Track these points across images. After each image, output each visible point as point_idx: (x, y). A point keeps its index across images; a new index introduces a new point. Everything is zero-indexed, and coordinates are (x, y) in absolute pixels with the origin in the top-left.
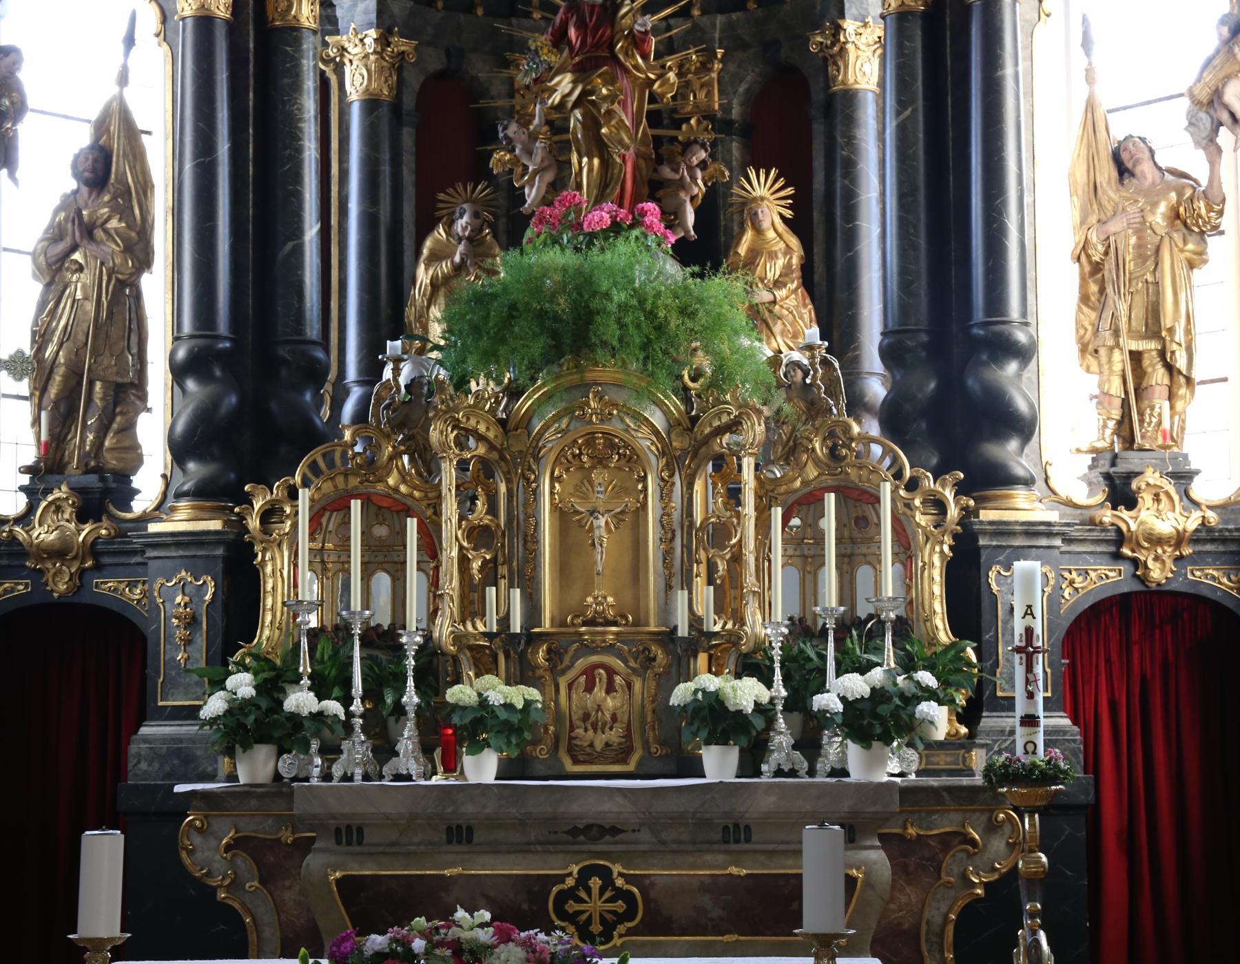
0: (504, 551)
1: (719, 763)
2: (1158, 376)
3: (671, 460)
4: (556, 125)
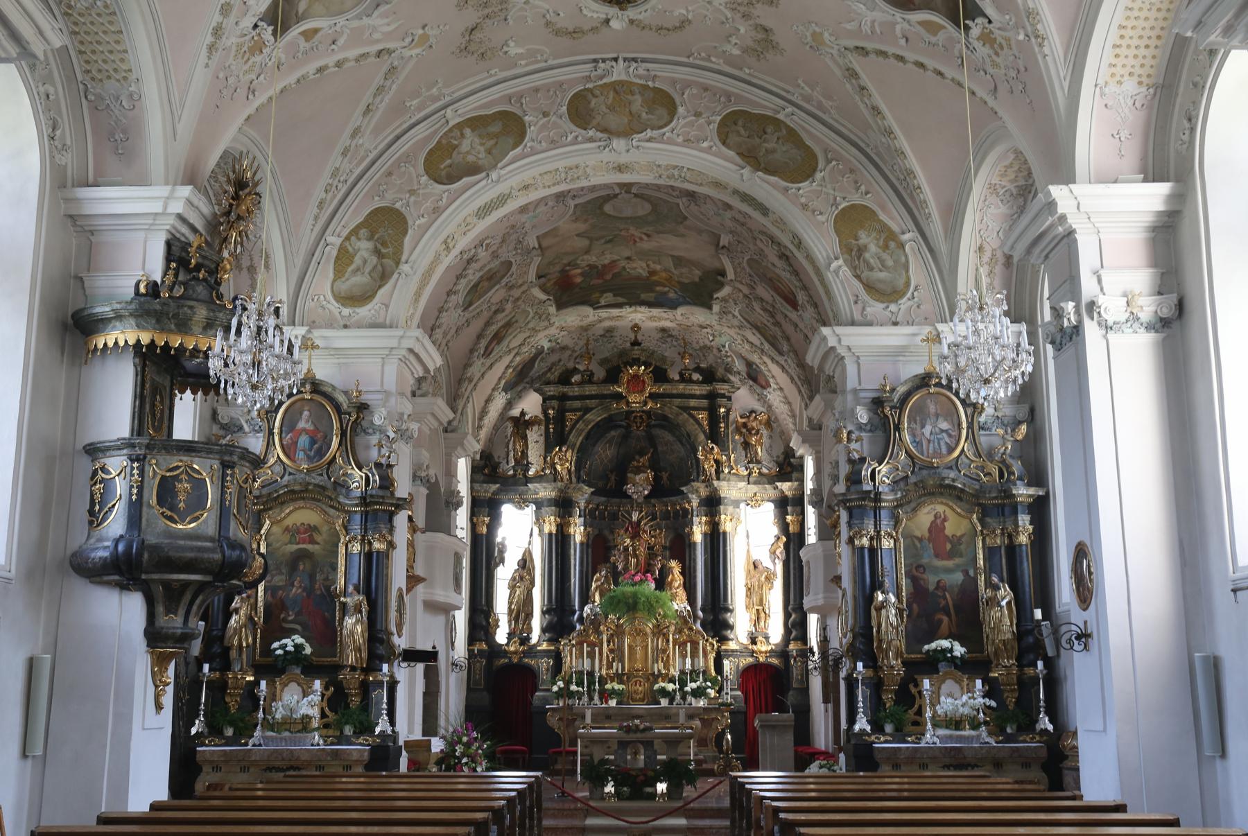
0: (617, 654)
1: (664, 702)
2: (762, 615)
3: (654, 634)
4: (626, 549)
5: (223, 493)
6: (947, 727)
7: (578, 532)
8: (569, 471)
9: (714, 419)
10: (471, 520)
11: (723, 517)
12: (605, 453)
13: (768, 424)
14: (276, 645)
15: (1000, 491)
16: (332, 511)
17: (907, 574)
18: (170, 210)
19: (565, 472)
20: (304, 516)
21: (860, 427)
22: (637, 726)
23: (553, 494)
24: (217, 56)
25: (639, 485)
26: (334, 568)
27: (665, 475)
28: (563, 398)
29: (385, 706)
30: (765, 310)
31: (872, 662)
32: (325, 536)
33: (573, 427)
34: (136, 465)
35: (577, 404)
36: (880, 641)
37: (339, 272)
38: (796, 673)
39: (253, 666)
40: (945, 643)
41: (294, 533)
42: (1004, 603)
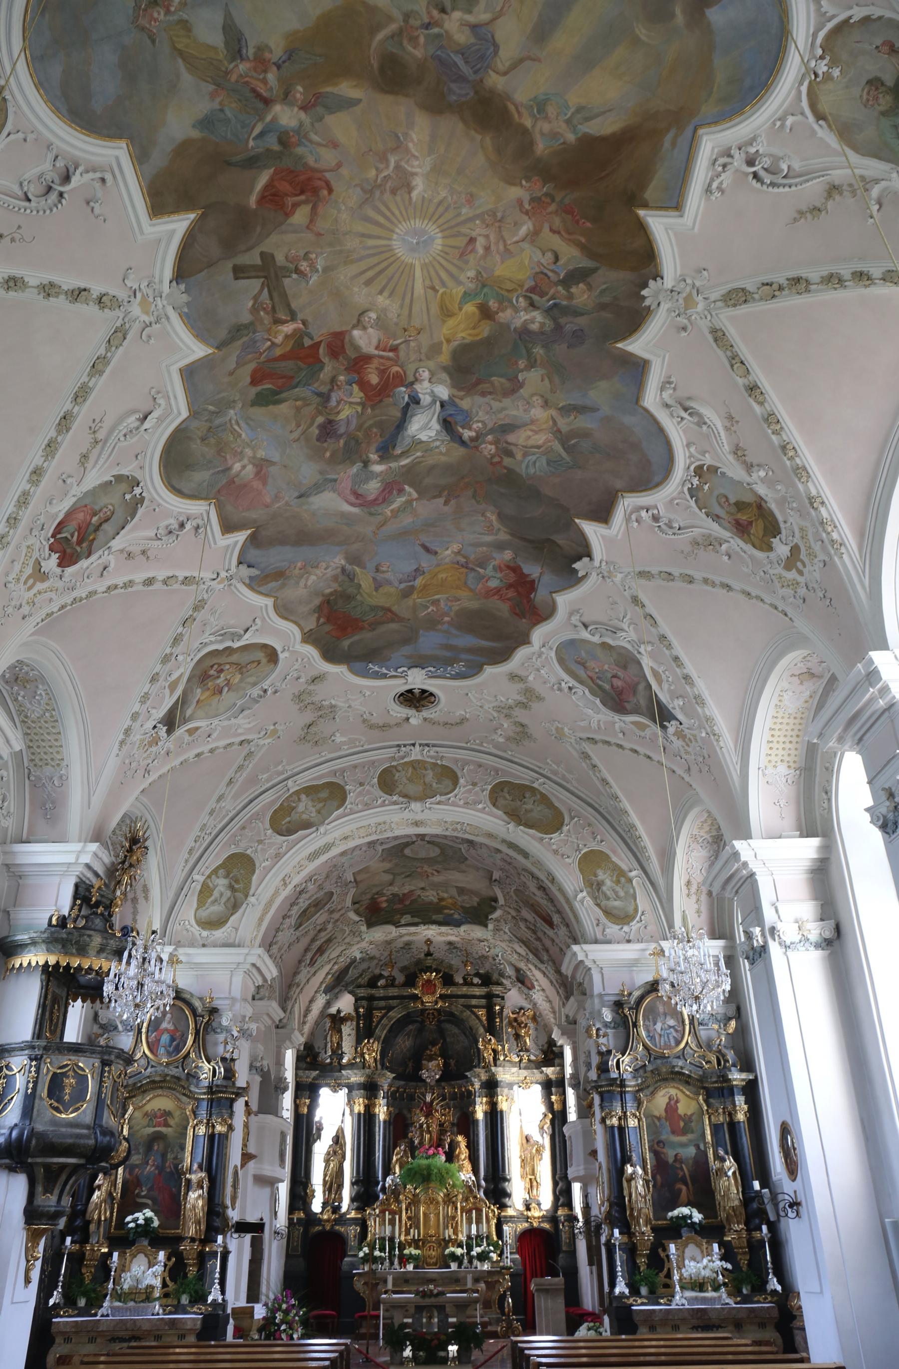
0: (414, 1220)
1: (454, 1266)
2: (535, 1184)
3: (445, 1202)
4: (421, 1126)
5: (101, 1087)
6: (693, 1290)
7: (382, 1112)
8: (375, 1060)
9: (491, 1015)
10: (295, 1102)
11: (500, 1098)
12: (404, 1043)
13: (534, 1018)
14: (129, 1219)
15: (719, 1077)
16: (184, 1099)
17: (650, 1148)
18: (80, 861)
19: (372, 1061)
20: (160, 1102)
21: (606, 1025)
22: (431, 1291)
23: (362, 1079)
24: (125, 748)
25: (432, 1071)
26: (183, 1148)
27: (452, 1062)
28: (371, 998)
29: (217, 1275)
30: (528, 928)
31: (626, 1230)
32: (177, 1119)
33: (379, 1022)
34: (34, 1063)
35: (382, 1003)
36: (632, 1209)
37: (201, 903)
38: (564, 1237)
40: (685, 1211)
41: (152, 1117)
42: (730, 1173)
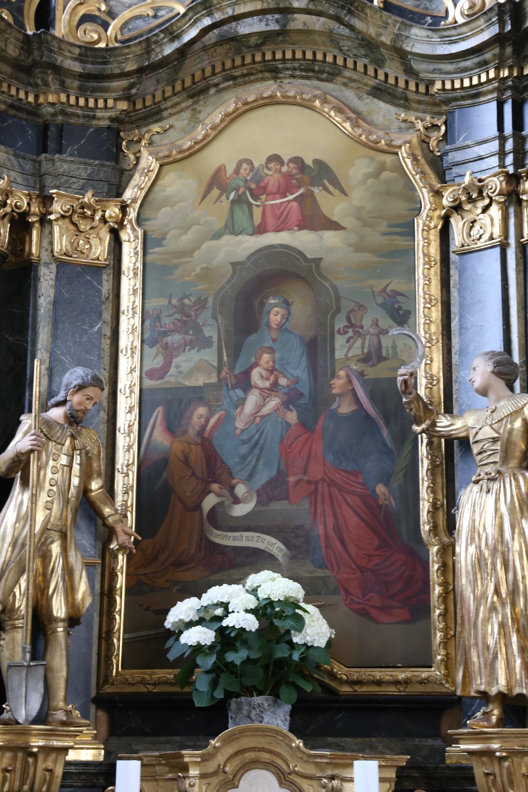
14: (183, 610)
16: (382, 111)
26: (403, 316)
32: (358, 196)
39: (102, 702)
41: (243, 193)
